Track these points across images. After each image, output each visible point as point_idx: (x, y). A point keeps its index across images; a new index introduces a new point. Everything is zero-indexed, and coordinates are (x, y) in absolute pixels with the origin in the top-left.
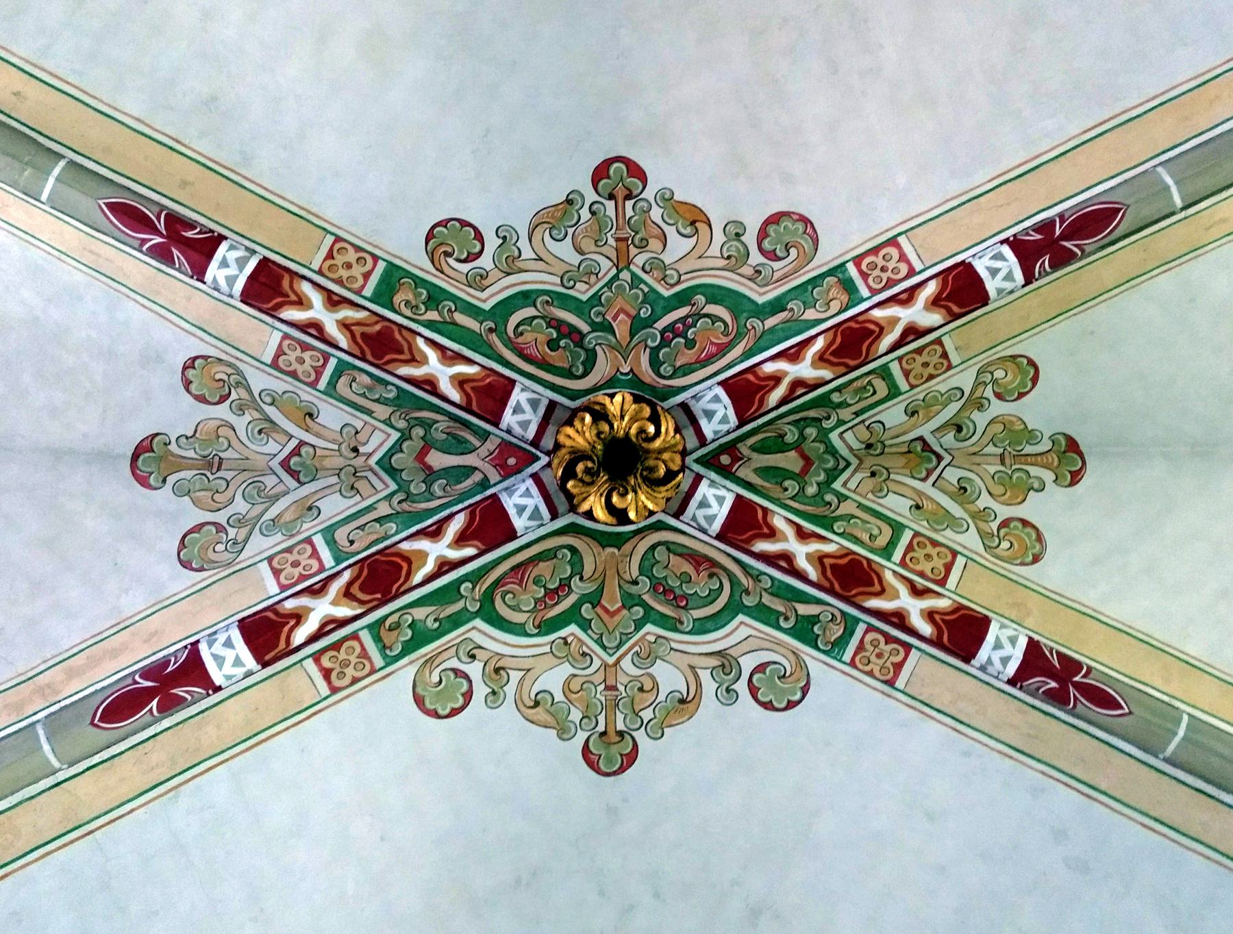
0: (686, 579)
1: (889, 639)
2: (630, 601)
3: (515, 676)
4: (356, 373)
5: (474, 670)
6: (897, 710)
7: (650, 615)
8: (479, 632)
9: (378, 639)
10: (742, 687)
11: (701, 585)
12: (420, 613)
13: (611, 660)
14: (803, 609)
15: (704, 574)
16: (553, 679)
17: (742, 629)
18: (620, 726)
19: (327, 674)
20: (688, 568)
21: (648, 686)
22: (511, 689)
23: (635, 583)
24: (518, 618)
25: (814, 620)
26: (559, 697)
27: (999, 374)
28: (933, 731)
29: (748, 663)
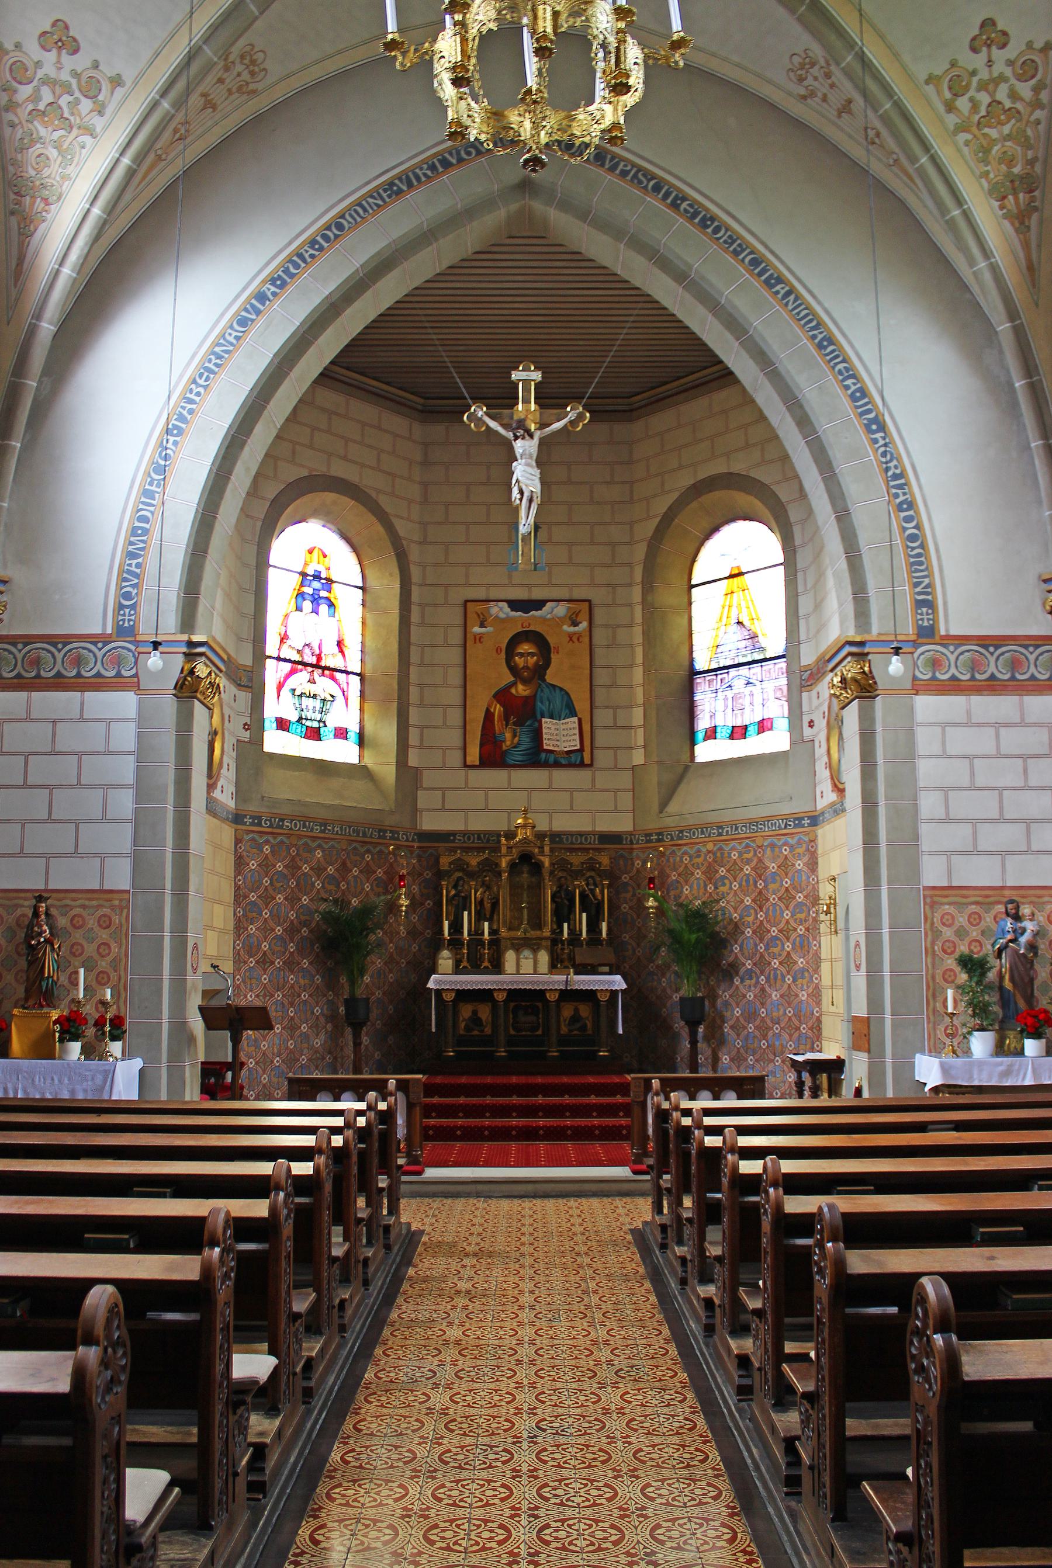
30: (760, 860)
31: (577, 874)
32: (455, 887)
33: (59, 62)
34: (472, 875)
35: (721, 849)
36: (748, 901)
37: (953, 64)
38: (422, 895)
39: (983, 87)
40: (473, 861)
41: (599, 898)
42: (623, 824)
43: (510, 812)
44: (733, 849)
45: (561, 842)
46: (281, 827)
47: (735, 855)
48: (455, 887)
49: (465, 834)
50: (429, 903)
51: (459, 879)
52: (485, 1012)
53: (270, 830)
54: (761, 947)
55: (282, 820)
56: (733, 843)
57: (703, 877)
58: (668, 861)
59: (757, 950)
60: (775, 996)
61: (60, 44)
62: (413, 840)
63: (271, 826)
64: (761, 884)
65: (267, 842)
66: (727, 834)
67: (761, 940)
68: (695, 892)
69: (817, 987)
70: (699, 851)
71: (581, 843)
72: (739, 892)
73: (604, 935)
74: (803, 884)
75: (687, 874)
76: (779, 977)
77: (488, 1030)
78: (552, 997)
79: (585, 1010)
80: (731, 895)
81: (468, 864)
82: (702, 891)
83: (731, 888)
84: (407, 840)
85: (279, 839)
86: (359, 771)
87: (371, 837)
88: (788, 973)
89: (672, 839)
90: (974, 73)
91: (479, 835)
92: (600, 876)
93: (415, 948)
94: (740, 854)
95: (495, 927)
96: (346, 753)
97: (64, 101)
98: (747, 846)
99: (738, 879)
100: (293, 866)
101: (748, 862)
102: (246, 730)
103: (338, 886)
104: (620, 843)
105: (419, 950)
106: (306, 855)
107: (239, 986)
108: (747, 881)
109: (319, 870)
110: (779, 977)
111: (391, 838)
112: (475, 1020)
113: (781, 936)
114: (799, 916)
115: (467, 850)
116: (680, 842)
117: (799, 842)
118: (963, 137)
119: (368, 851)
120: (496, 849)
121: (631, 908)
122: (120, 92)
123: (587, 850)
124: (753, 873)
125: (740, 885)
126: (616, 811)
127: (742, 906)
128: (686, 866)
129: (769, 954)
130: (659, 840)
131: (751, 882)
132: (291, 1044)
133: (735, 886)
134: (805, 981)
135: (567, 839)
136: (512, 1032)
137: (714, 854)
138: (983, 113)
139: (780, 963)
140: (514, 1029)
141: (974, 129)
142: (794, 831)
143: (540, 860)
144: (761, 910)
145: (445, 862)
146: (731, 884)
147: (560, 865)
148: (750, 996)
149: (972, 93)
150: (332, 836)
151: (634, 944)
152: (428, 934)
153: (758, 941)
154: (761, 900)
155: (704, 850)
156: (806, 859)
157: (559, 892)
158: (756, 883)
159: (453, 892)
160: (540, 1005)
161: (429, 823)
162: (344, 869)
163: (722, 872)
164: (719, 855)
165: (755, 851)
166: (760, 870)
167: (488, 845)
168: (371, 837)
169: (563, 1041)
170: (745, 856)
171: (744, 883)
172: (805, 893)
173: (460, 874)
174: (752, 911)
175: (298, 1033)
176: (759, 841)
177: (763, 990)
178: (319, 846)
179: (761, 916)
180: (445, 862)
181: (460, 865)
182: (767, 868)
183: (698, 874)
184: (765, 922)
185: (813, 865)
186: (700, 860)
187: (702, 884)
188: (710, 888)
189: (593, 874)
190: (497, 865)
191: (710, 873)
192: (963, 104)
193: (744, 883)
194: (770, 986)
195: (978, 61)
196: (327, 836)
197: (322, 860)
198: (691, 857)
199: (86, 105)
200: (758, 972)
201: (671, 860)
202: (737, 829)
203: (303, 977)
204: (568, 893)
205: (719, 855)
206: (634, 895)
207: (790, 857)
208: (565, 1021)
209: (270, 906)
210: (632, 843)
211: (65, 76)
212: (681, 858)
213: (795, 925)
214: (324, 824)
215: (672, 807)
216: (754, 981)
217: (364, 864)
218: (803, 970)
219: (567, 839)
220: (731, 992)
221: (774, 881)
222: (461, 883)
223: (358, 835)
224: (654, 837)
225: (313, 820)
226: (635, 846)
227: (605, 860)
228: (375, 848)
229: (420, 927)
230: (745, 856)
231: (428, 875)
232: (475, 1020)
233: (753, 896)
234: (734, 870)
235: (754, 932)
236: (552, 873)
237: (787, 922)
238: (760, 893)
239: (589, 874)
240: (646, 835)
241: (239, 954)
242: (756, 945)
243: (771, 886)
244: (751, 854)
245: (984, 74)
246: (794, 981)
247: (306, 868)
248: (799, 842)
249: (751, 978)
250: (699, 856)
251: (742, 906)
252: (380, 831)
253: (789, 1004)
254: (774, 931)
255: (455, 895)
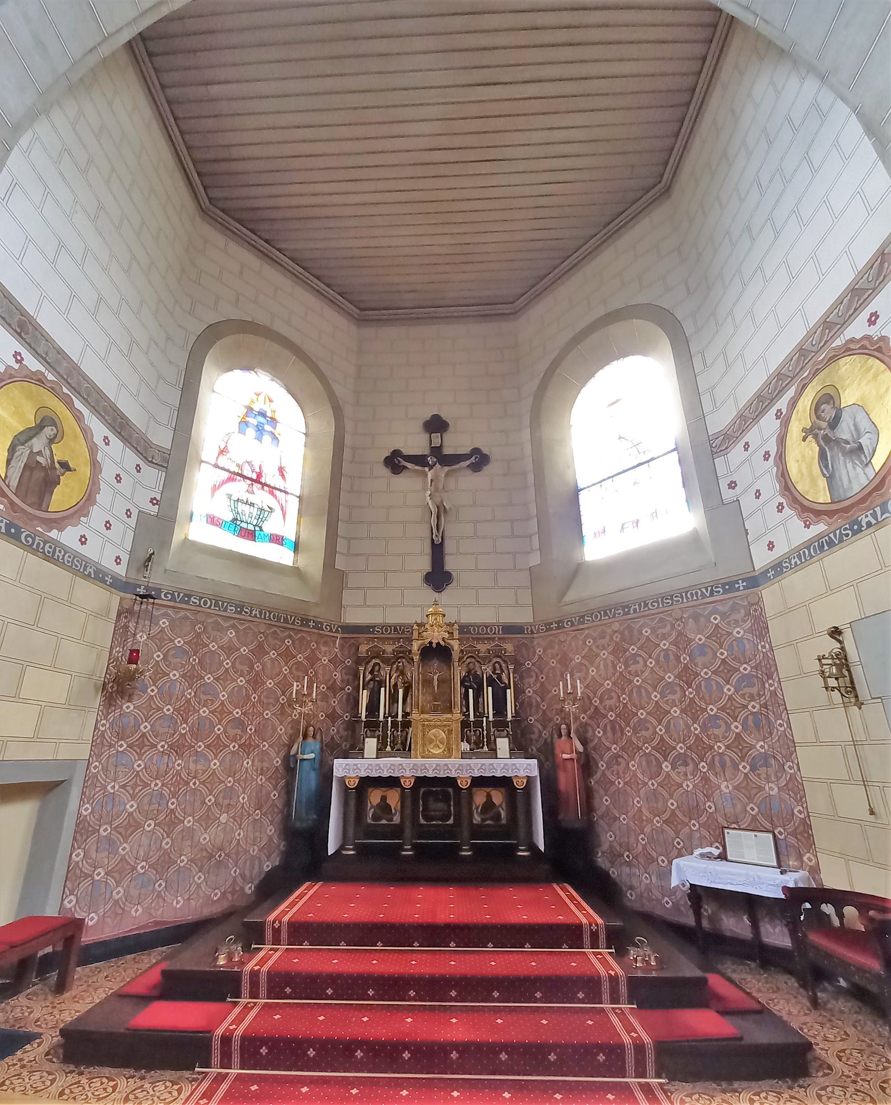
30: (680, 634)
31: (485, 660)
32: (371, 672)
34: (388, 661)
35: (629, 627)
36: (670, 677)
38: (342, 681)
40: (389, 648)
41: (507, 682)
42: (523, 616)
43: (422, 607)
44: (644, 625)
45: (469, 632)
46: (187, 603)
47: (646, 631)
48: (371, 672)
49: (385, 627)
50: (349, 689)
51: (375, 665)
52: (393, 798)
53: (171, 604)
54: (696, 728)
55: (189, 596)
56: (642, 621)
57: (611, 657)
58: (570, 645)
59: (689, 731)
60: (725, 787)
62: (337, 631)
63: (173, 599)
64: (685, 659)
65: (165, 615)
66: (635, 610)
67: (695, 720)
68: (602, 671)
69: (793, 777)
70: (604, 632)
71: (487, 633)
72: (656, 669)
73: (509, 718)
74: (748, 653)
75: (591, 657)
76: (729, 763)
77: (397, 819)
78: (464, 784)
79: (498, 797)
80: (646, 674)
81: (384, 651)
82: (611, 671)
83: (645, 665)
84: (331, 631)
85: (182, 614)
86: (295, 571)
87: (293, 624)
88: (742, 759)
89: (573, 625)
91: (396, 628)
92: (505, 662)
93: (333, 731)
94: (653, 630)
95: (408, 710)
96: (284, 556)
98: (662, 620)
99: (654, 655)
100: (197, 644)
101: (664, 637)
102: (154, 504)
103: (252, 667)
104: (523, 633)
105: (338, 732)
106: (215, 633)
107: (95, 776)
108: (666, 657)
109: (230, 649)
110: (729, 763)
111: (314, 627)
112: (384, 807)
113: (723, 715)
114: (747, 690)
115: (383, 640)
116: (582, 627)
117: (734, 609)
119: (290, 637)
120: (410, 640)
121: (534, 692)
123: (493, 639)
124: (673, 648)
125: (657, 661)
126: (517, 605)
127: (663, 683)
128: (590, 649)
129: (709, 737)
130: (558, 628)
131: (672, 657)
132: (166, 844)
133: (651, 663)
134: (771, 771)
135: (474, 630)
136: (422, 821)
137: (622, 634)
139: (727, 747)
140: (424, 818)
142: (724, 597)
143: (449, 644)
144: (690, 686)
145: (363, 649)
146: (645, 662)
147: (470, 654)
148: (688, 785)
150: (249, 618)
151: (540, 727)
152: (347, 717)
153: (690, 721)
154: (687, 676)
155: (609, 631)
156: (748, 624)
157: (468, 676)
158: (678, 658)
159: (369, 677)
160: (450, 790)
161: (354, 616)
162: (260, 651)
163: (633, 649)
164: (626, 633)
165: (673, 626)
166: (682, 641)
167: (403, 636)
168: (293, 624)
169: (477, 832)
170: (660, 631)
171: (662, 659)
172: (753, 663)
173: (378, 661)
174: (678, 689)
175: (179, 828)
176: (677, 614)
177: (705, 779)
178: (233, 626)
179: (690, 693)
180: (363, 649)
181: (376, 654)
182: (690, 641)
183: (604, 654)
184: (697, 700)
185: (761, 629)
186: (604, 641)
187: (610, 664)
188: (621, 667)
189: (498, 660)
190: (410, 652)
191: (618, 651)
193: (662, 659)
194: (716, 774)
196: (242, 617)
197: (235, 640)
198: (594, 639)
200: (694, 756)
201: (573, 644)
202: (646, 605)
203: (195, 762)
204: (476, 676)
205: (626, 633)
206: (537, 679)
207: (723, 625)
208: (477, 808)
209: (160, 683)
210: (532, 632)
212: (584, 642)
213: (744, 702)
214: (240, 607)
215: (571, 596)
216: (690, 767)
217: (284, 648)
218: (765, 757)
219: (474, 630)
220: (659, 779)
221: (703, 654)
222: (377, 668)
223: (279, 620)
224: (555, 625)
225: (230, 602)
226: (535, 635)
227: (509, 647)
228: (296, 634)
229: (339, 711)
230: (660, 631)
231: (349, 662)
232: (384, 807)
233: (676, 672)
234: (648, 647)
235: (683, 711)
236: (460, 659)
237: (730, 698)
238: (686, 667)
239: (495, 660)
240: (546, 625)
241: (103, 736)
242: (688, 727)
243: (700, 660)
244: (669, 627)
246: (753, 769)
247: (213, 646)
248: (734, 609)
249: (687, 765)
250: (604, 637)
251: (663, 683)
252: (302, 620)
253: (751, 799)
254: (712, 710)
255: (371, 680)
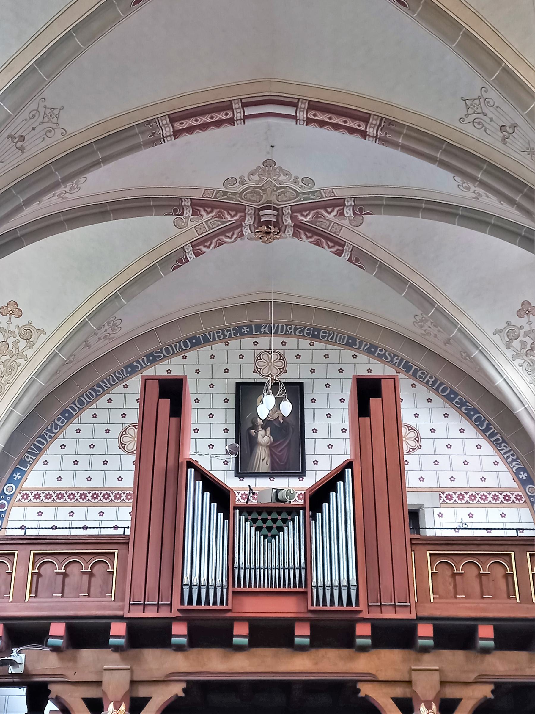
0: (252, 197)
1: (207, 197)
2: (265, 190)
3: (292, 180)
4: (325, 228)
5: (301, 184)
6: (203, 186)
7: (260, 188)
8: (300, 190)
9: (322, 195)
10: (238, 180)
11: (249, 196)
12: (312, 197)
13: (269, 179)
14: (226, 197)
15: (248, 198)
16: (282, 178)
17: (239, 191)
18: (267, 167)
19: (333, 192)
20: (251, 198)
21: (260, 176)
22: (293, 178)
23: (264, 194)
24: (290, 190)
25: (223, 196)
26: (282, 174)
27: (183, 224)
28: (196, 184)
29: (238, 184)
33: (10, 321)
37: (508, 323)
39: (526, 334)
61: (11, 312)
90: (521, 327)
97: (11, 340)
118: (518, 362)
122: (43, 338)
138: (529, 348)
141: (525, 357)
149: (521, 338)
192: (516, 344)
195: (523, 322)
199: (23, 344)
211: (12, 328)
245: (527, 328)
